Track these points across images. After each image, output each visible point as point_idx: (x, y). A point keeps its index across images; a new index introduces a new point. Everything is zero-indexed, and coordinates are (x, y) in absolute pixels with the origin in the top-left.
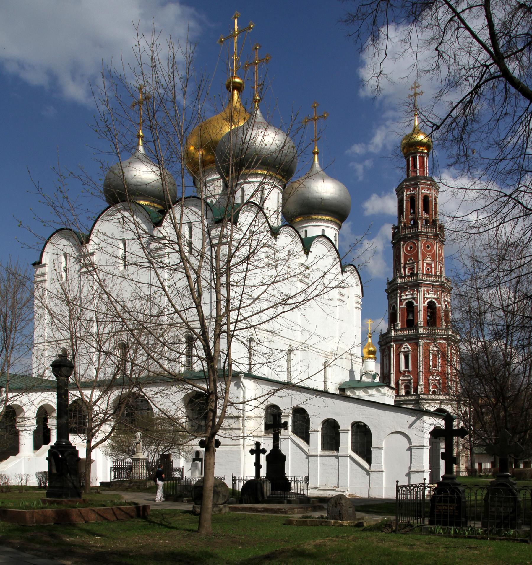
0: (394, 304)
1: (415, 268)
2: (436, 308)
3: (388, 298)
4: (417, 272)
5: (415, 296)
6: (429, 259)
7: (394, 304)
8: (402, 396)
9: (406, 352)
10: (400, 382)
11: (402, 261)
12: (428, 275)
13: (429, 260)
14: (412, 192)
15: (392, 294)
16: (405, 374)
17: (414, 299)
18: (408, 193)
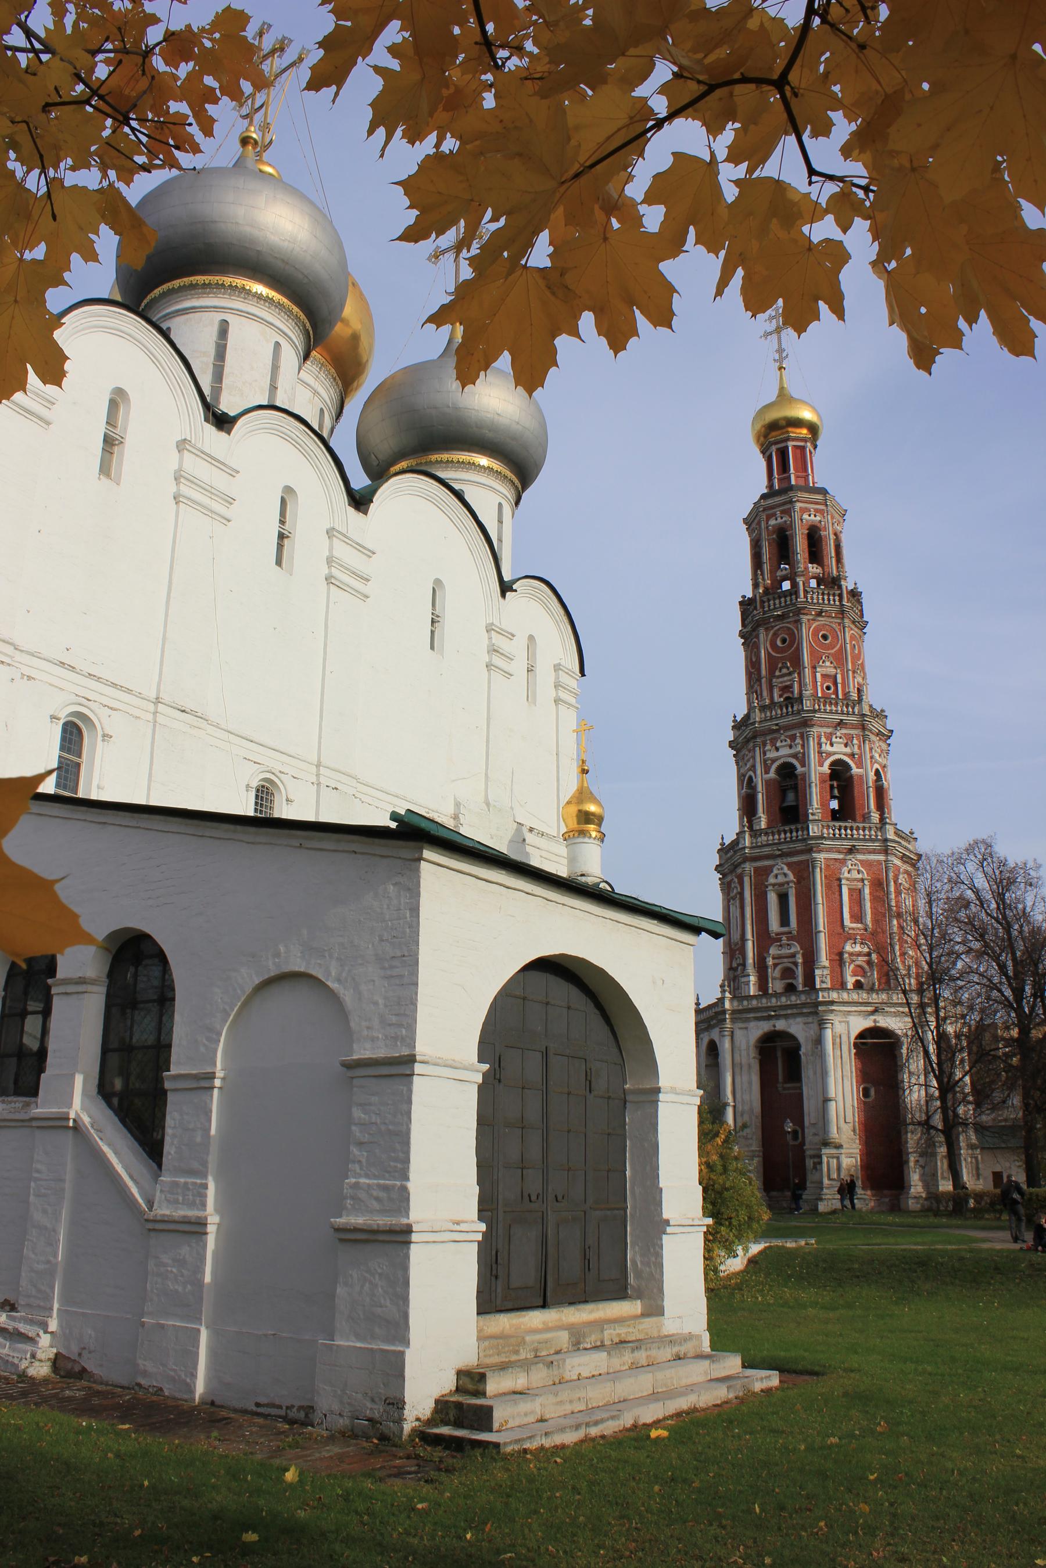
0: (751, 773)
1: (796, 685)
2: (851, 776)
3: (737, 763)
4: (801, 691)
5: (799, 748)
6: (828, 664)
7: (751, 773)
8: (776, 995)
9: (781, 885)
10: (770, 962)
11: (764, 672)
12: (826, 700)
13: (827, 667)
14: (779, 520)
15: (745, 751)
16: (780, 940)
17: (795, 756)
18: (772, 522)
